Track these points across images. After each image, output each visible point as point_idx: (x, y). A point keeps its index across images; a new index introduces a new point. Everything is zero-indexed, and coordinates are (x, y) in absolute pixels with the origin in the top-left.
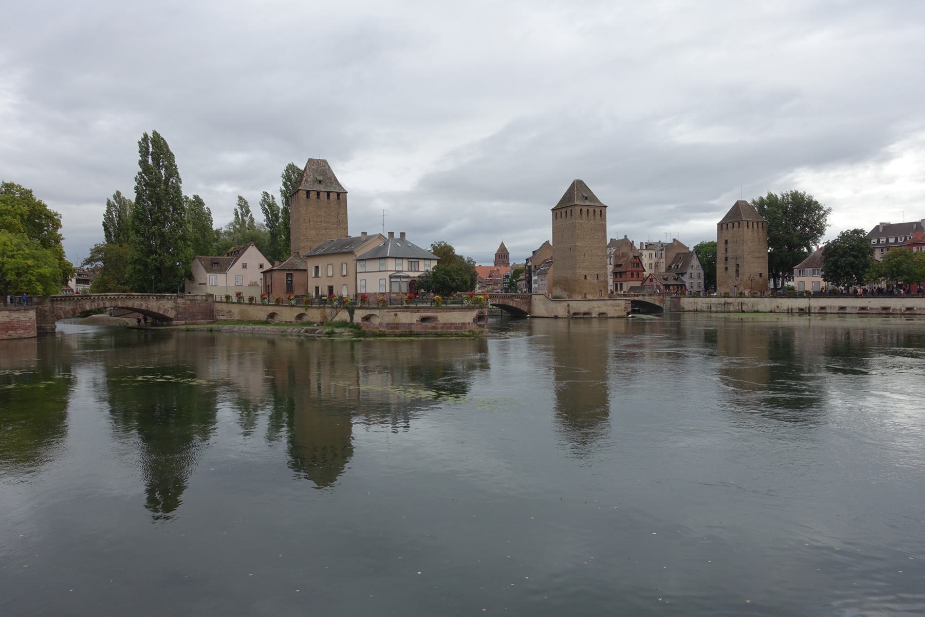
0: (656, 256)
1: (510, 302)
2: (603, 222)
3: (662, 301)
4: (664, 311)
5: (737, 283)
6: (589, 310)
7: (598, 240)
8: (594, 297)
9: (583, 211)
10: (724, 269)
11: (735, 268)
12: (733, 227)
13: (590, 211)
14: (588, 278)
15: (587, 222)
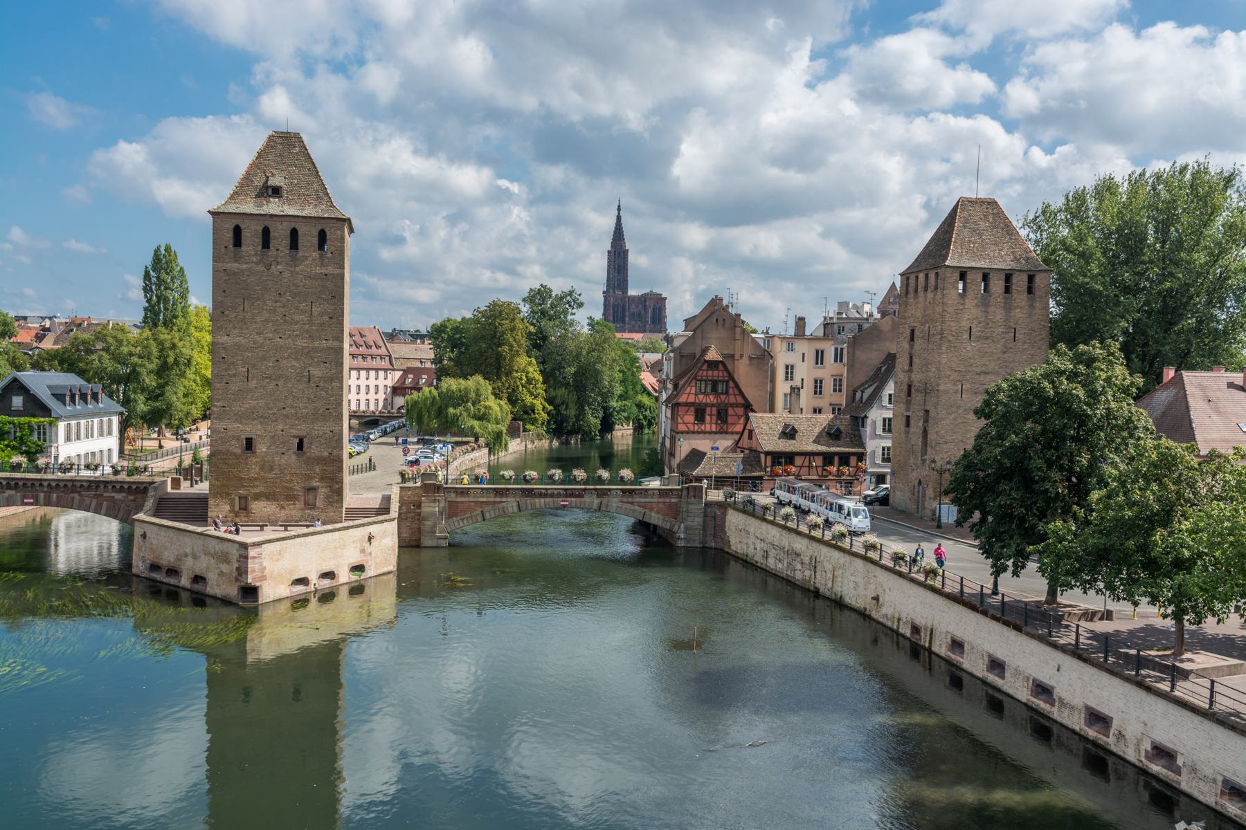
0: (838, 357)
1: (87, 501)
2: (331, 269)
5: (924, 472)
6: (178, 559)
7: (307, 327)
9: (246, 234)
10: (904, 419)
11: (921, 423)
12: (926, 289)
13: (272, 234)
14: (261, 448)
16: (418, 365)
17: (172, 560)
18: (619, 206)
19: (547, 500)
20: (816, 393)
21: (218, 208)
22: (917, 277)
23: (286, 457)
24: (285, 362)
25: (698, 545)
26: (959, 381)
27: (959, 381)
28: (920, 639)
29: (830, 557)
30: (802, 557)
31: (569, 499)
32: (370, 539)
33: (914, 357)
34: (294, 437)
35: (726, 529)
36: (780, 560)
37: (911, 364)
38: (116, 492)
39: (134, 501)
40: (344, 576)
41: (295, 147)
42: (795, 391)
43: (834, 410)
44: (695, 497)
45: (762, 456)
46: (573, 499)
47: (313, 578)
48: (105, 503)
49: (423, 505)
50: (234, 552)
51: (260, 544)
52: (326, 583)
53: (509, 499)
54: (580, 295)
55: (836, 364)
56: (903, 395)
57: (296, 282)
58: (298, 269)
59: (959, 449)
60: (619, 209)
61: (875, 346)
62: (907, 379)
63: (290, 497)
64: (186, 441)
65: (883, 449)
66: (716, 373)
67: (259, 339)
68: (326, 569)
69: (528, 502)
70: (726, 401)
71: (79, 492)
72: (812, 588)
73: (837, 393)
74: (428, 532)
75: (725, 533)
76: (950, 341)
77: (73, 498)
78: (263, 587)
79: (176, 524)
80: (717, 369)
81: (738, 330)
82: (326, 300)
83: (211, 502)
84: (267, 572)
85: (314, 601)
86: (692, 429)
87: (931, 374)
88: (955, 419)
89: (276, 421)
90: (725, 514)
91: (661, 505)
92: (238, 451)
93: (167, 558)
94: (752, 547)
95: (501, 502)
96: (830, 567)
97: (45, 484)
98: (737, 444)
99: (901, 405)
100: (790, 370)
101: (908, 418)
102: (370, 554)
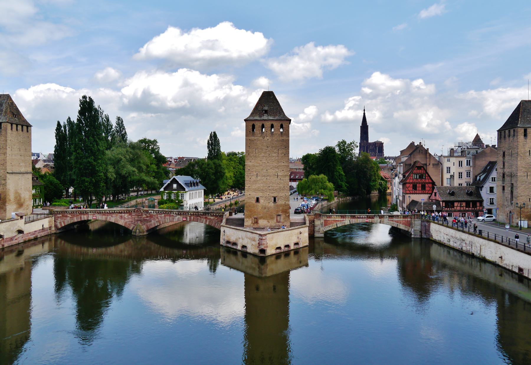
0: (468, 163)
1: (202, 219)
3: (410, 224)
4: (413, 236)
5: (511, 208)
6: (236, 240)
7: (277, 158)
8: (269, 222)
10: (502, 188)
11: (510, 189)
12: (509, 136)
14: (261, 201)
15: (261, 138)
16: (295, 170)
17: (234, 240)
18: (364, 109)
19: (360, 219)
20: (459, 178)
21: (247, 118)
22: (505, 132)
23: (270, 204)
24: (270, 170)
25: (418, 237)
26: (526, 172)
27: (526, 172)
28: (523, 274)
29: (479, 241)
30: (466, 241)
31: (368, 219)
32: (300, 233)
33: (505, 163)
34: (273, 197)
35: (431, 231)
36: (455, 243)
37: (504, 166)
38: (211, 216)
39: (217, 219)
40: (292, 247)
41: (271, 96)
42: (452, 177)
43: (467, 184)
44: (417, 218)
45: (441, 203)
46: (370, 219)
47: (283, 247)
48: (208, 220)
49: (315, 221)
50: (257, 237)
51: (265, 235)
52: (287, 249)
53: (346, 219)
54: (357, 143)
55: (467, 166)
56: (501, 178)
57: (273, 142)
58: (274, 138)
59: (527, 199)
60: (364, 111)
61: (483, 159)
62: (502, 171)
63: (272, 218)
64: (222, 199)
65: (490, 199)
66: (420, 171)
67: (261, 163)
68: (287, 244)
69: (353, 220)
70: (425, 182)
71: (200, 217)
72: (471, 253)
73: (468, 178)
74: (317, 231)
75: (430, 232)
76: (521, 156)
77: (198, 218)
78: (267, 250)
79: (238, 228)
80: (421, 169)
81: (428, 154)
82: (284, 149)
83: (245, 220)
84: (268, 245)
85: (283, 256)
86: (412, 193)
87: (513, 169)
88: (525, 187)
89: (267, 191)
90: (430, 225)
91: (404, 222)
92: (254, 202)
93: (232, 239)
94: (443, 238)
95: (343, 220)
96: (479, 246)
97: (190, 213)
98: (429, 198)
99: (500, 182)
100: (449, 169)
101: (504, 187)
102: (301, 238)
